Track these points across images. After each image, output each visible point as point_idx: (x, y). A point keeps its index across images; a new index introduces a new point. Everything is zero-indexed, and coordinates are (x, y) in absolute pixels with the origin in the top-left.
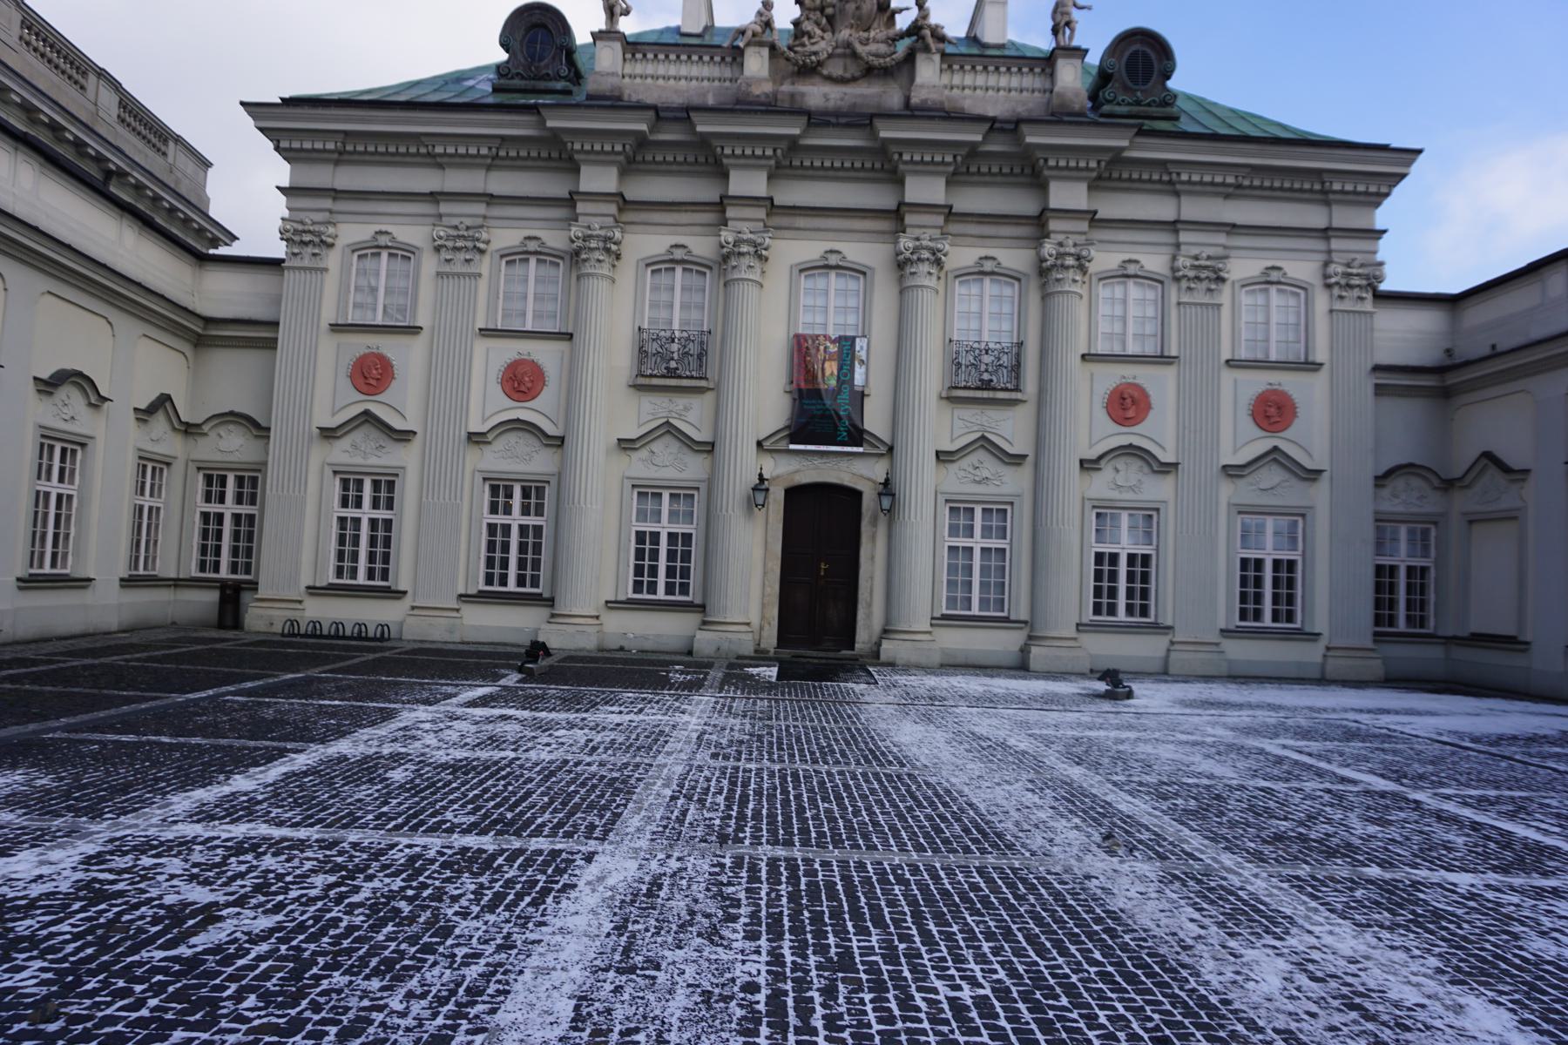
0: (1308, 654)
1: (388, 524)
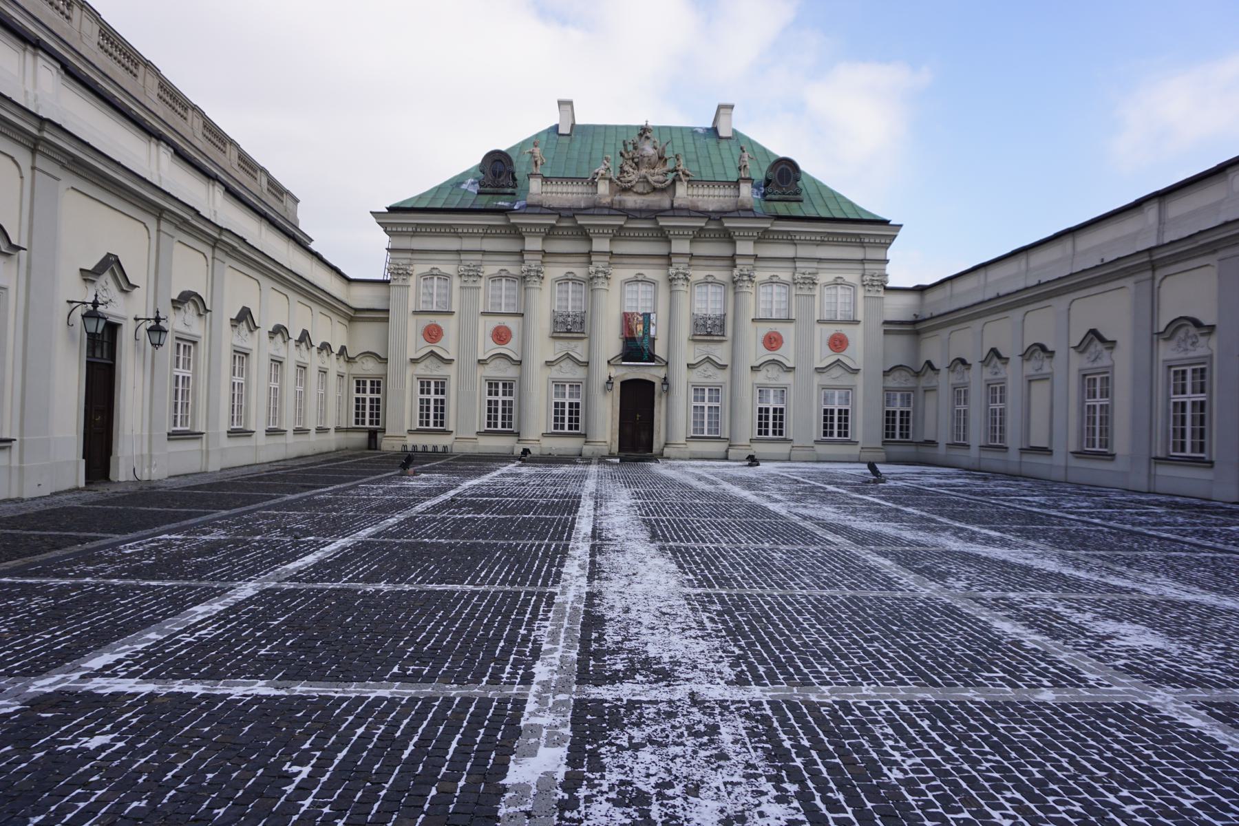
0: (854, 451)
1: (442, 401)
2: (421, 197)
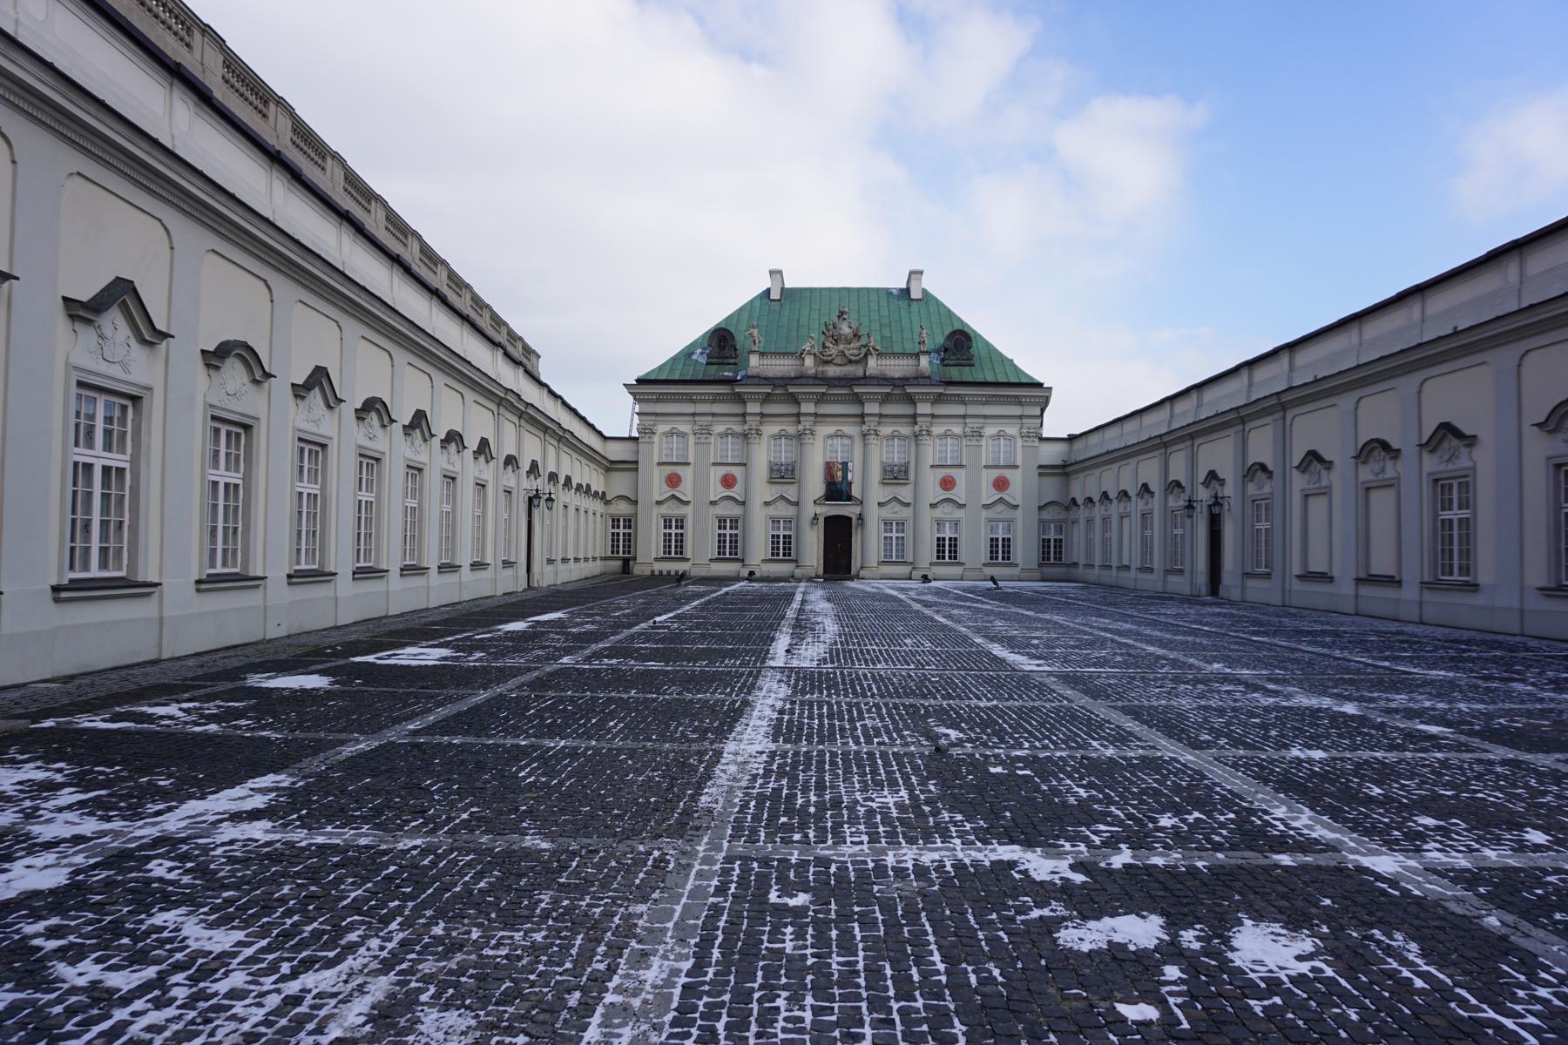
0: (1015, 571)
2: (661, 368)
